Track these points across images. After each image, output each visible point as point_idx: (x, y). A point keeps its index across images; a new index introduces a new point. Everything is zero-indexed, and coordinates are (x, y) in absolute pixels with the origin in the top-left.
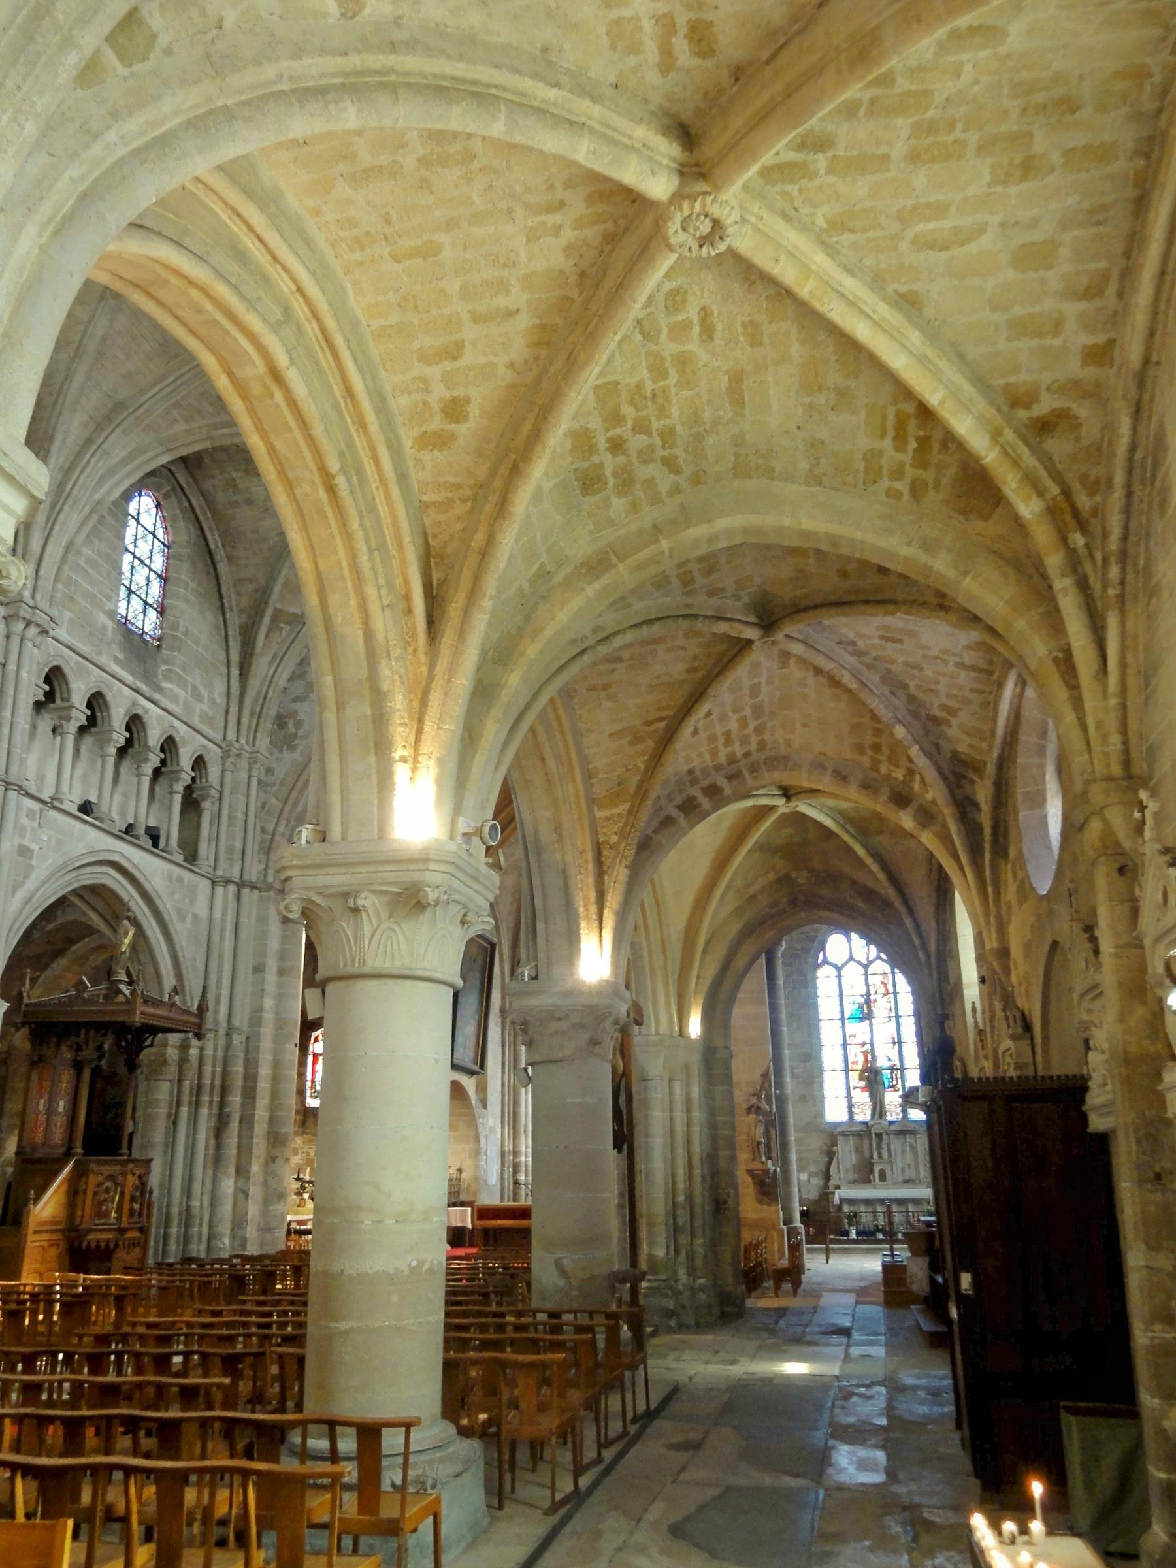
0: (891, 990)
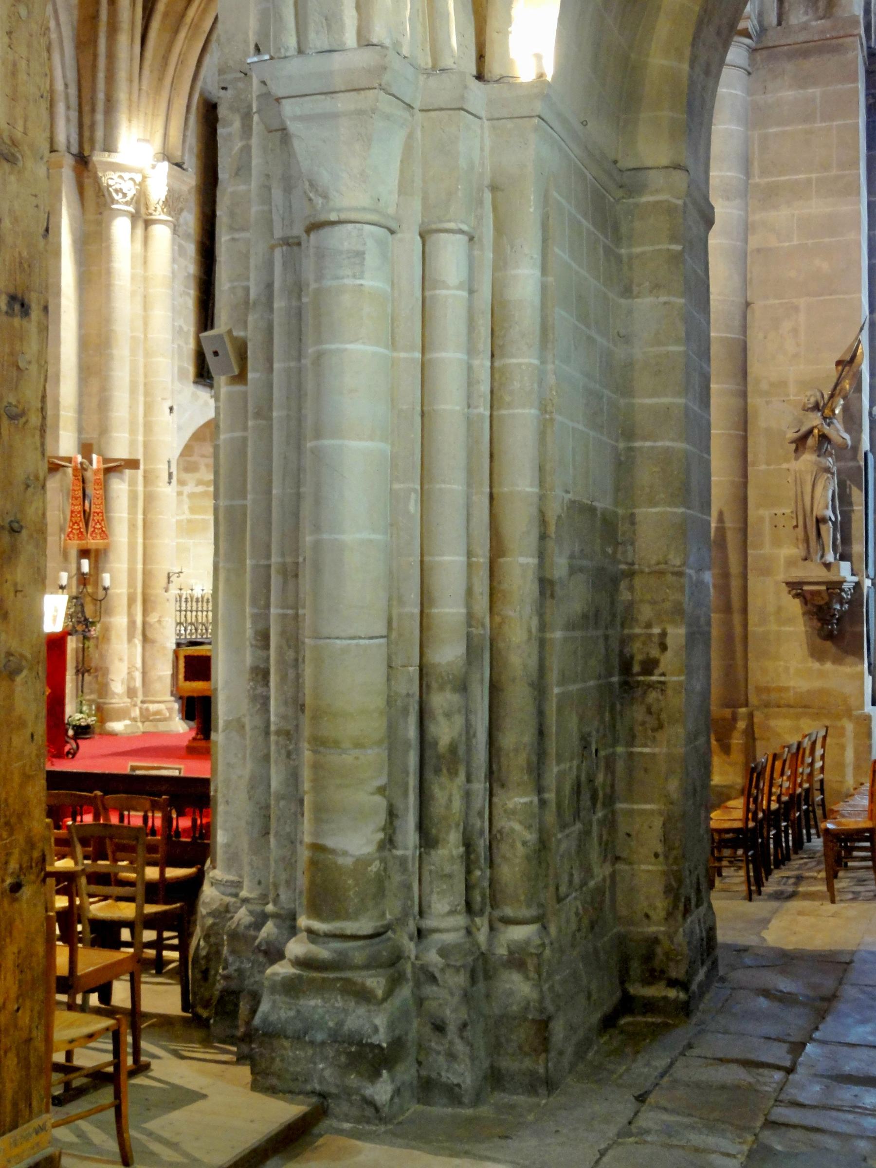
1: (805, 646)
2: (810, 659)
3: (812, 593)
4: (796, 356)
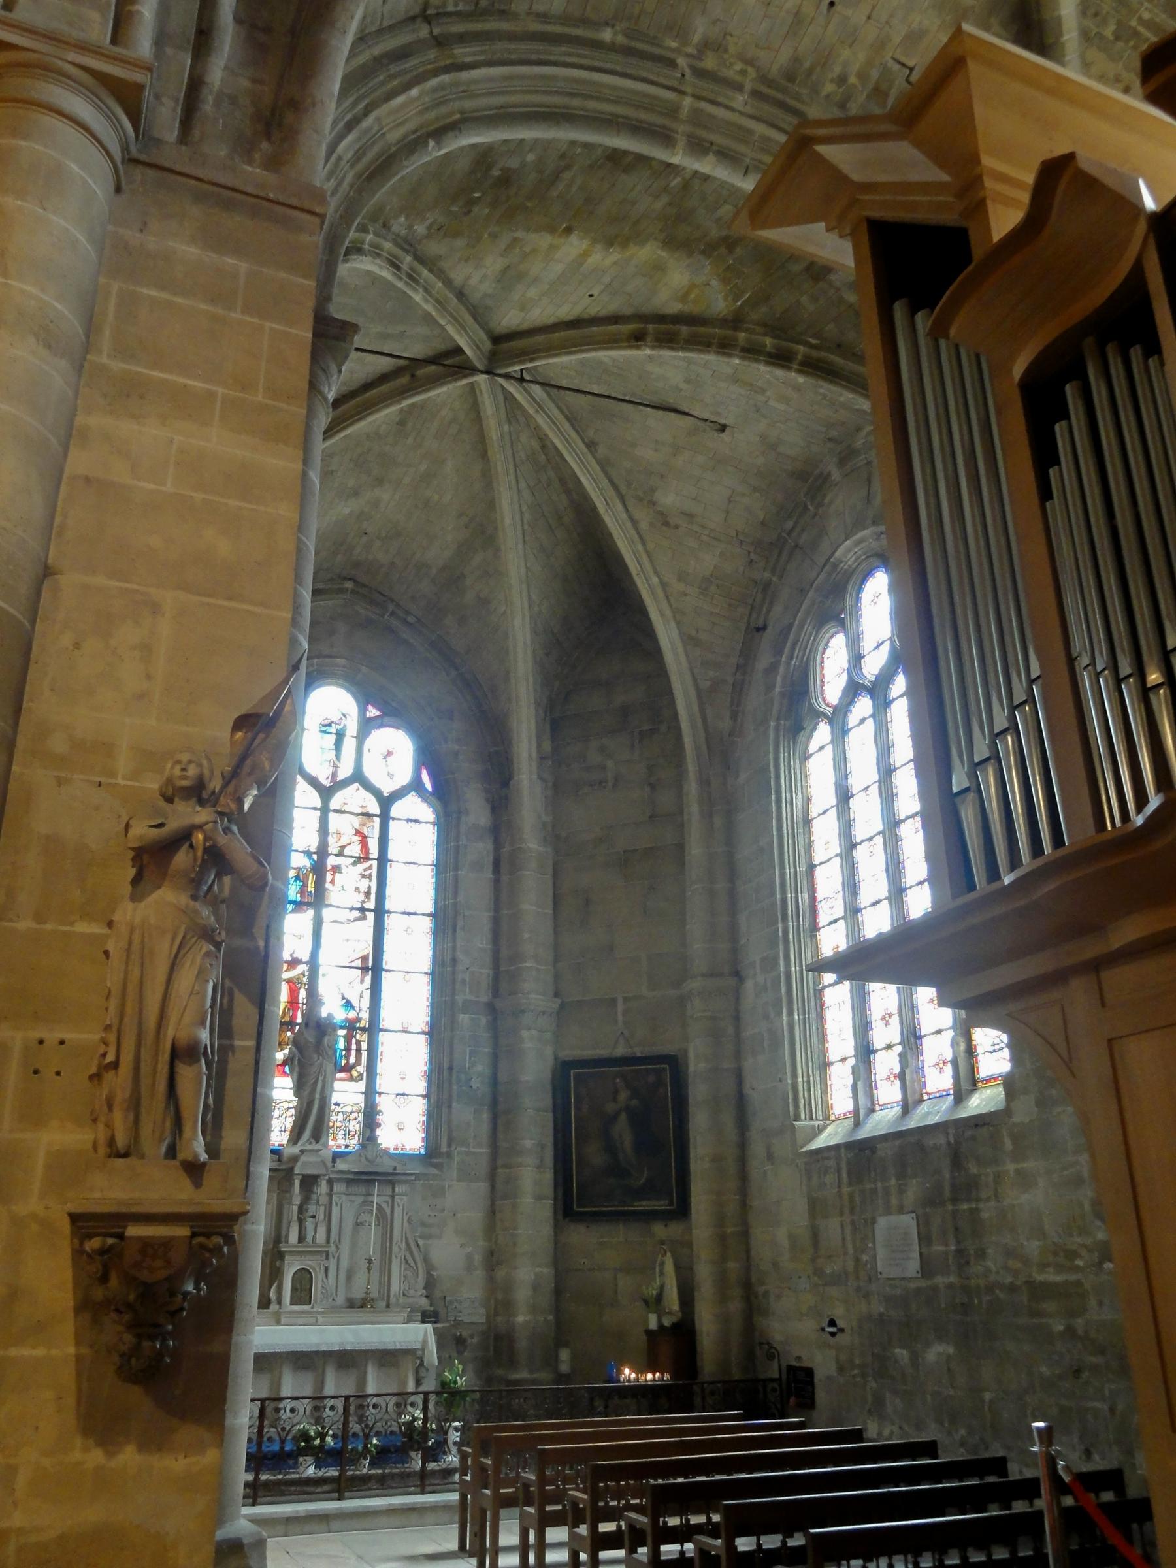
0: (374, 851)
1: (71, 1401)
2: (78, 1441)
3: (146, 1245)
4: (141, 696)
